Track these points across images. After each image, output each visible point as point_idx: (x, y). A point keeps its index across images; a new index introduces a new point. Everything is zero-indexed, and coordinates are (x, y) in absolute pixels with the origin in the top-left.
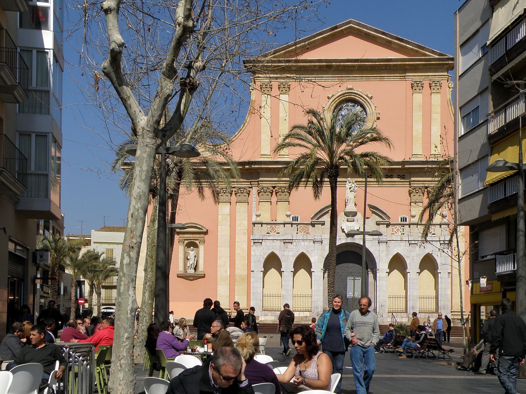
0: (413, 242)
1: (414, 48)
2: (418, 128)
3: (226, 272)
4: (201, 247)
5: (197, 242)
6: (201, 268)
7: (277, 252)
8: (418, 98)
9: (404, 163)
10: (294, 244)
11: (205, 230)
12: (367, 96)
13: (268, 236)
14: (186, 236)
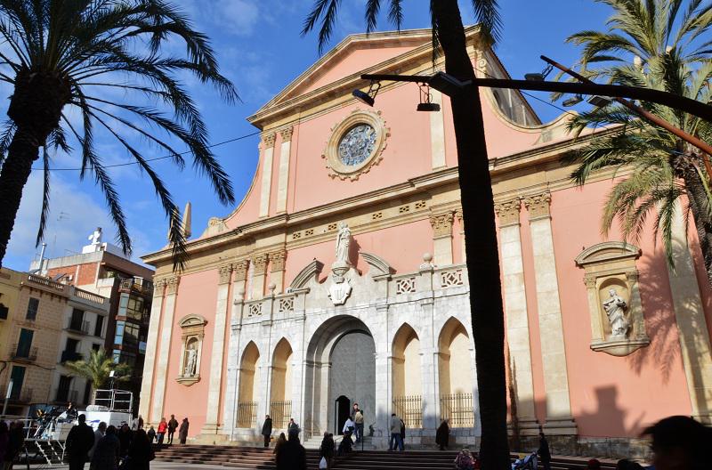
0: (425, 302)
5: (196, 337)
9: (411, 182)
10: (275, 326)
12: (374, 113)
14: (190, 330)
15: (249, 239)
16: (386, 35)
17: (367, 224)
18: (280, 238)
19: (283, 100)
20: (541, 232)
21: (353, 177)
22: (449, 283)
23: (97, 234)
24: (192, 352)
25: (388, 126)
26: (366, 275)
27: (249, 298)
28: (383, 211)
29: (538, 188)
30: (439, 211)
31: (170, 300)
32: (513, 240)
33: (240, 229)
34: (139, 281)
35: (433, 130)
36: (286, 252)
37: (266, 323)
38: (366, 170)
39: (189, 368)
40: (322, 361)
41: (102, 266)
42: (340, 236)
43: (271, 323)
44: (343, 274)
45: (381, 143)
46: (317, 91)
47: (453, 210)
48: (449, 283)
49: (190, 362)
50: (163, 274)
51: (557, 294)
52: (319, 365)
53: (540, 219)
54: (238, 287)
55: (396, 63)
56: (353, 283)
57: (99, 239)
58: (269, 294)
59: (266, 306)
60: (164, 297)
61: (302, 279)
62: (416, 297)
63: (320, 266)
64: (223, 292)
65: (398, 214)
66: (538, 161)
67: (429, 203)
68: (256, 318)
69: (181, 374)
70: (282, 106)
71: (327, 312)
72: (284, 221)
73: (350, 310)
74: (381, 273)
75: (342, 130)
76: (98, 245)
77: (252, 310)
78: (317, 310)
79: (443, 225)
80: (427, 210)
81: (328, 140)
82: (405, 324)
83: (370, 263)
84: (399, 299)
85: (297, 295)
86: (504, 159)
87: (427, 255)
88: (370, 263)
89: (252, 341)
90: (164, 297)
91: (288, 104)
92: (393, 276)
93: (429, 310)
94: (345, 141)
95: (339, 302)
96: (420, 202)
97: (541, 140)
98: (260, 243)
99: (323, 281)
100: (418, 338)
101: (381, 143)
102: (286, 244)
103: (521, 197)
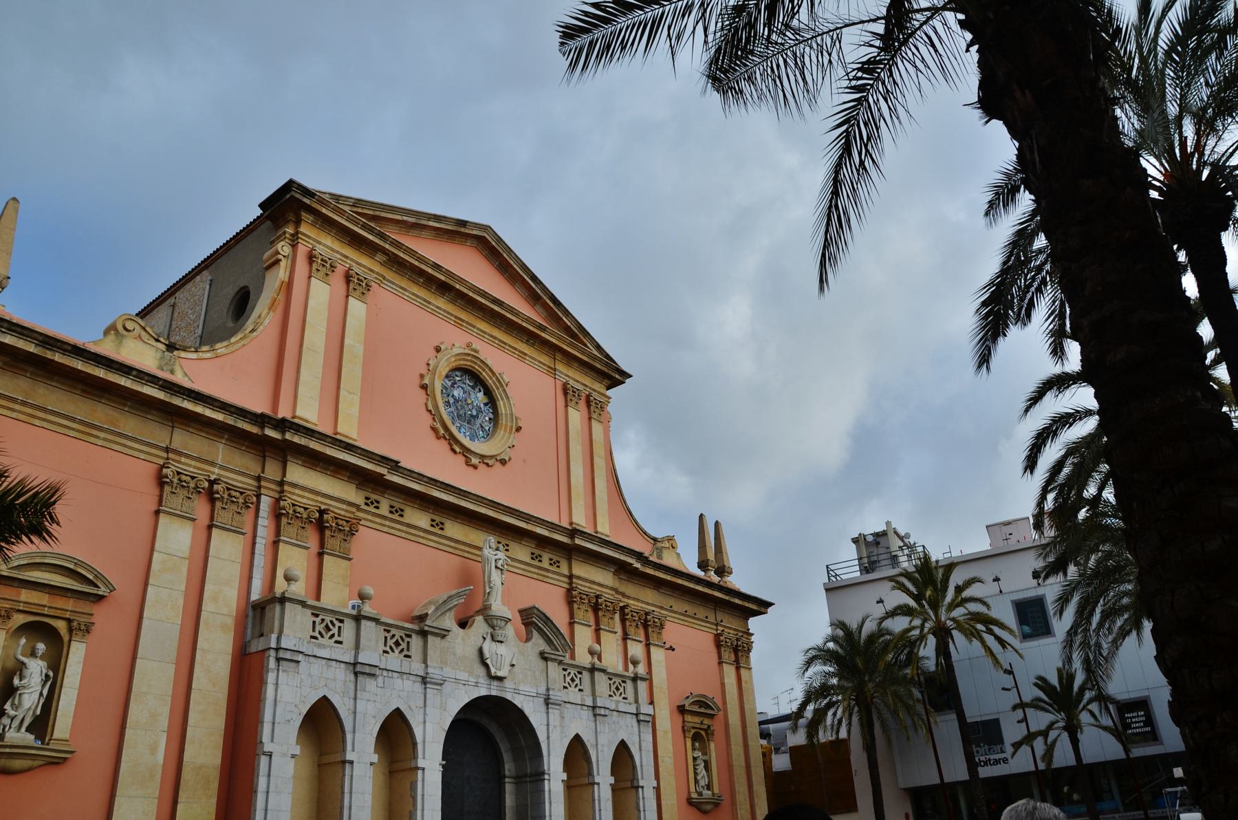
3: (153, 751)
4: (77, 653)
6: (62, 726)
7: (336, 700)
10: (380, 679)
11: (102, 590)
14: (26, 595)
18: (349, 492)
30: (583, 587)
74: (548, 649)
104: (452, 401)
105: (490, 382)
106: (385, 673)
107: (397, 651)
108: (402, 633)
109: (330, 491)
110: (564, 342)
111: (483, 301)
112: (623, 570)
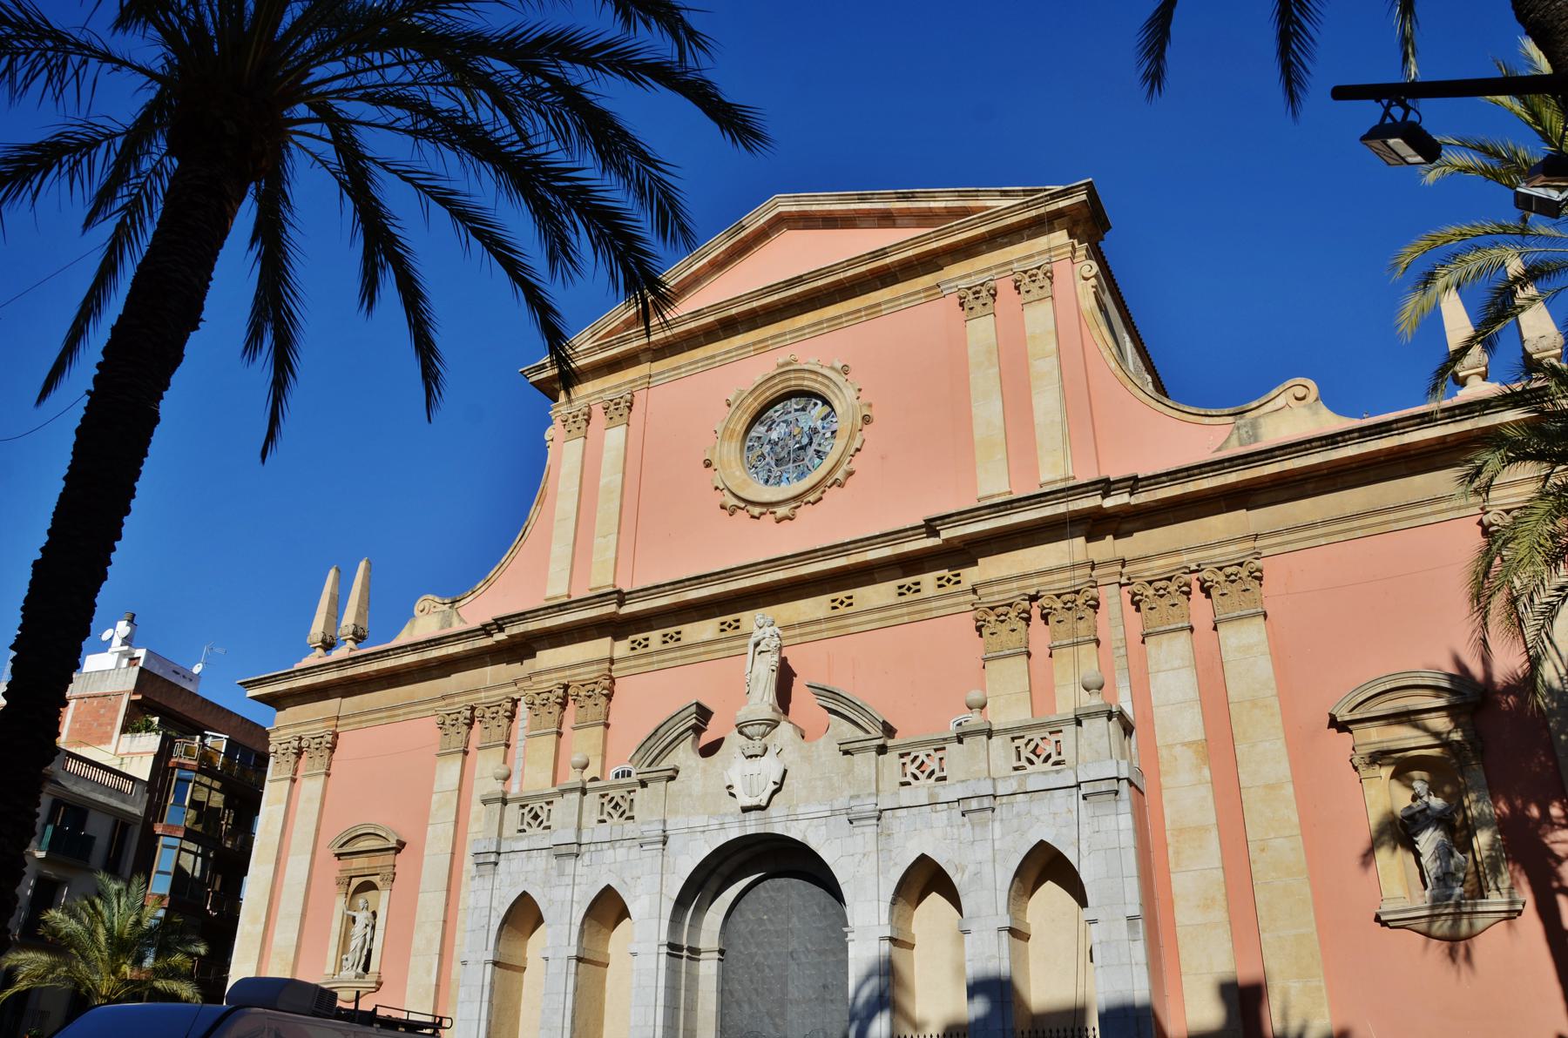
0: (974, 804)
1: (950, 204)
2: (988, 412)
3: (429, 972)
8: (982, 330)
9: (930, 527)
10: (586, 858)
11: (393, 844)
12: (832, 368)
13: (522, 839)
14: (359, 863)
15: (521, 649)
16: (862, 199)
17: (818, 622)
18: (599, 648)
19: (610, 334)
20: (1246, 647)
21: (782, 511)
22: (1031, 762)
23: (123, 628)
24: (362, 917)
25: (865, 399)
26: (822, 741)
27: (514, 789)
28: (858, 593)
29: (1232, 548)
30: (995, 595)
31: (311, 788)
32: (1177, 663)
33: (500, 624)
34: (218, 742)
35: (977, 410)
36: (613, 681)
37: (564, 850)
38: (812, 498)
39: (354, 955)
40: (702, 945)
41: (132, 703)
42: (757, 645)
43: (571, 852)
44: (764, 735)
45: (851, 437)
46: (697, 314)
47: (1032, 592)
48: (1031, 762)
49: (355, 942)
50: (284, 727)
51: (1289, 790)
52: (695, 952)
53: (1240, 618)
54: (487, 765)
55: (888, 261)
56: (791, 758)
57: (127, 641)
58: (574, 778)
59: (563, 812)
60: (294, 780)
61: (658, 744)
62: (948, 792)
63: (704, 714)
64: (449, 772)
65: (893, 599)
66: (1442, 440)
67: (970, 576)
68: (536, 837)
69: (329, 969)
70: (610, 345)
71: (722, 827)
72: (612, 608)
73: (778, 823)
75: (754, 405)
76: (122, 654)
77: (528, 818)
78: (699, 821)
79: (1006, 627)
80: (964, 592)
81: (719, 427)
82: (923, 859)
83: (831, 711)
84: (906, 796)
85: (643, 784)
86: (1155, 480)
87: (975, 695)
88: (831, 711)
89: (524, 894)
90: (294, 780)
91: (623, 341)
92: (890, 743)
93: (984, 825)
94: (759, 430)
95: (749, 802)
96: (945, 573)
97: (1234, 440)
98: (547, 658)
99: (709, 750)
100: (953, 897)
101: (851, 437)
102: (612, 661)
103: (1194, 567)
104: (767, 448)
105: (816, 387)
106: (593, 847)
107: (616, 816)
108: (623, 792)
109: (1052, 563)
110: (952, 233)
111: (776, 297)
112: (1095, 525)
